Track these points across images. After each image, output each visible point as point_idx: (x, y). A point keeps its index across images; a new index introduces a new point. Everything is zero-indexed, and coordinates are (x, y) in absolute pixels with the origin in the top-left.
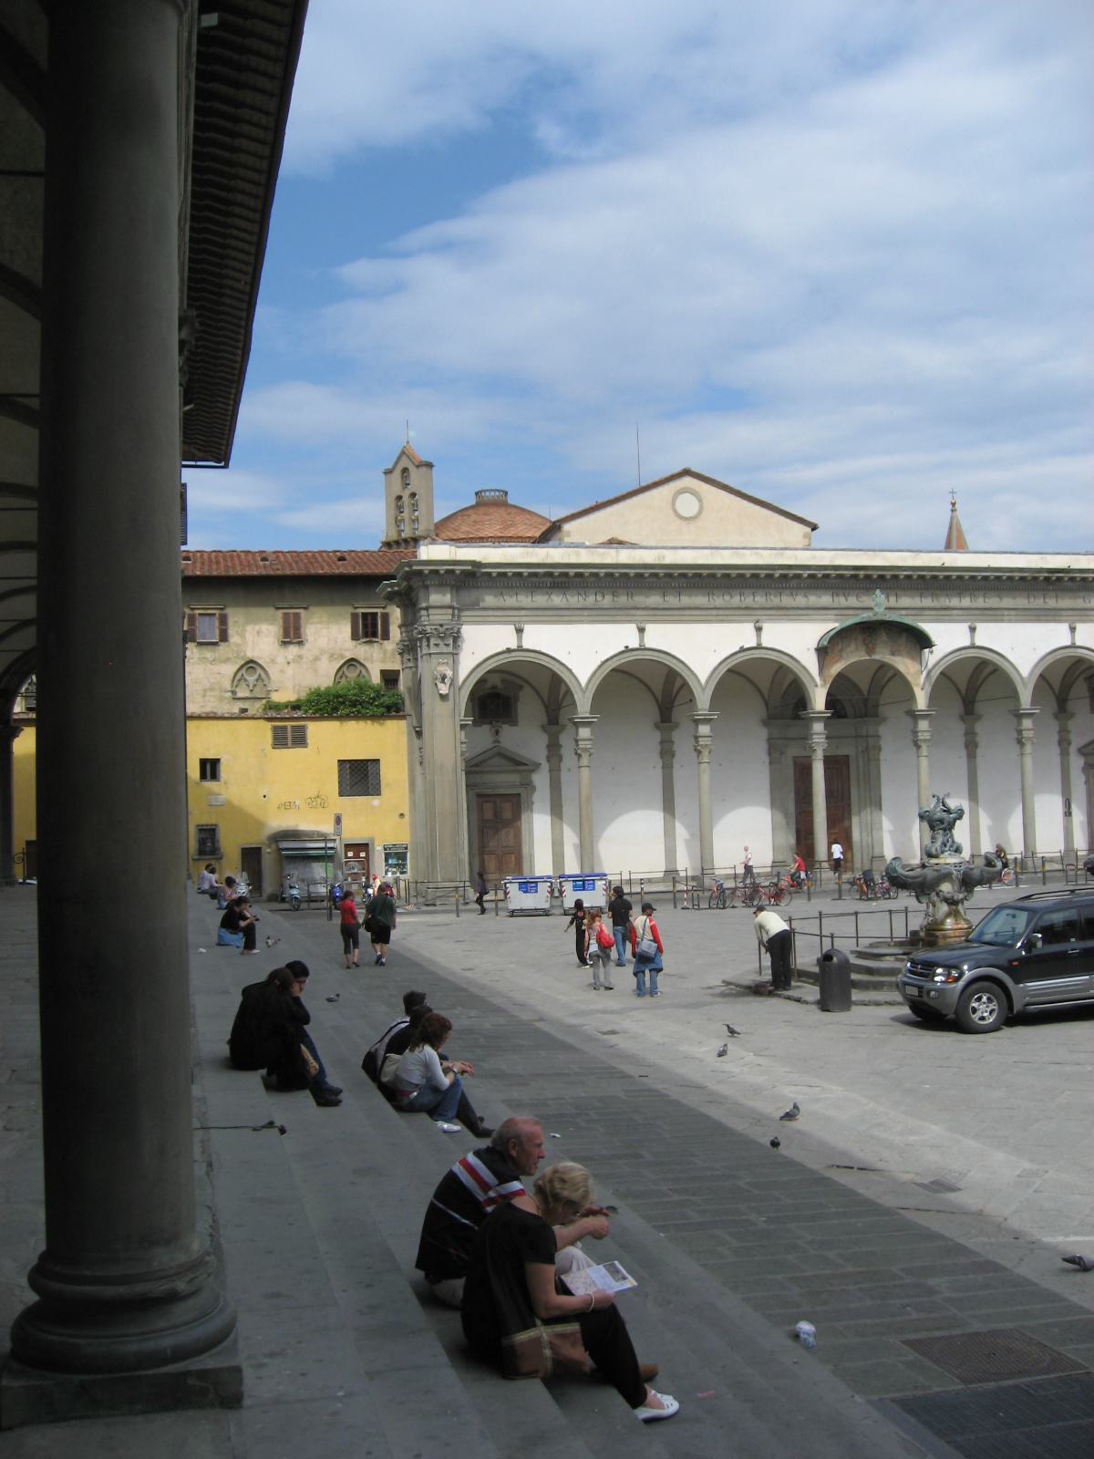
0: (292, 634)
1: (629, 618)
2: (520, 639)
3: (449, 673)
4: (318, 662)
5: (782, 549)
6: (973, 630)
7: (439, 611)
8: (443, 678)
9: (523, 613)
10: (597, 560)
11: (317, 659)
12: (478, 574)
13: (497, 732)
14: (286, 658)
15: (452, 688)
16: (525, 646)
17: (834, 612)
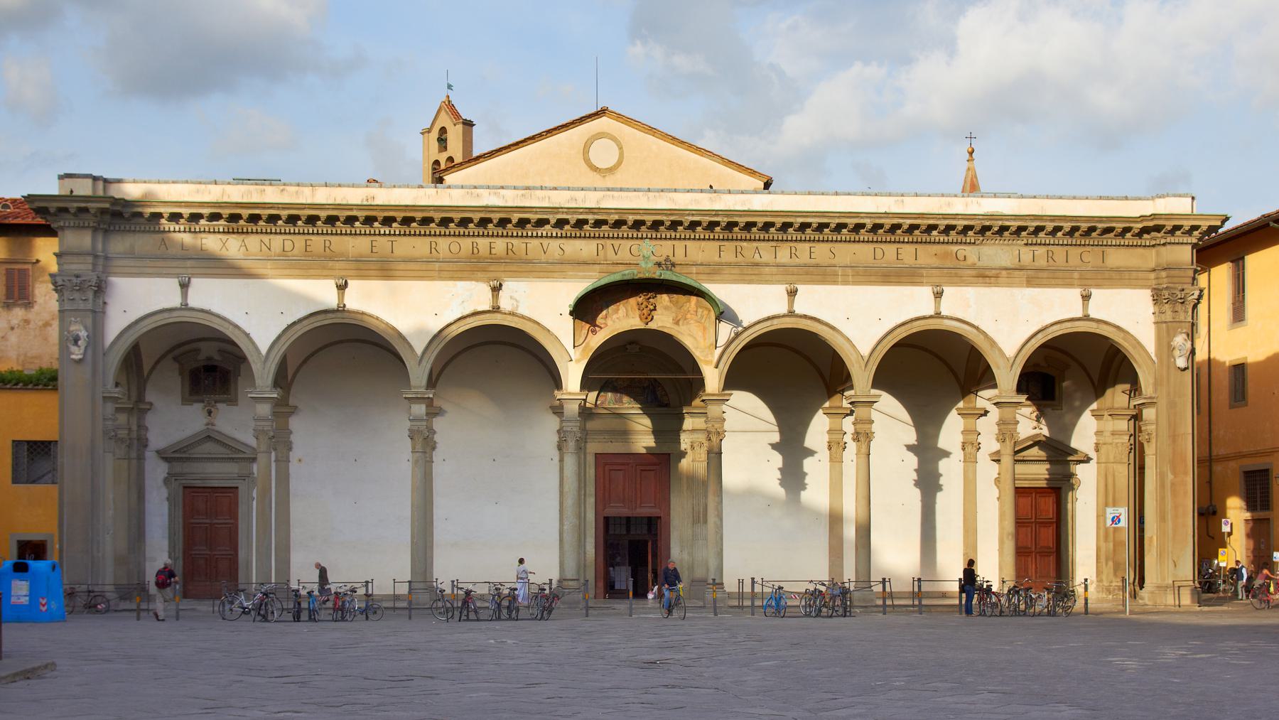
0: (16, 294)
1: (325, 272)
2: (185, 295)
3: (83, 334)
4: (49, 328)
5: (528, 188)
6: (792, 293)
7: (75, 259)
8: (76, 340)
9: (189, 263)
10: (255, 199)
11: (47, 324)
12: (126, 216)
13: (210, 413)
14: (9, 322)
15: (90, 352)
16: (193, 302)
17: (597, 267)
